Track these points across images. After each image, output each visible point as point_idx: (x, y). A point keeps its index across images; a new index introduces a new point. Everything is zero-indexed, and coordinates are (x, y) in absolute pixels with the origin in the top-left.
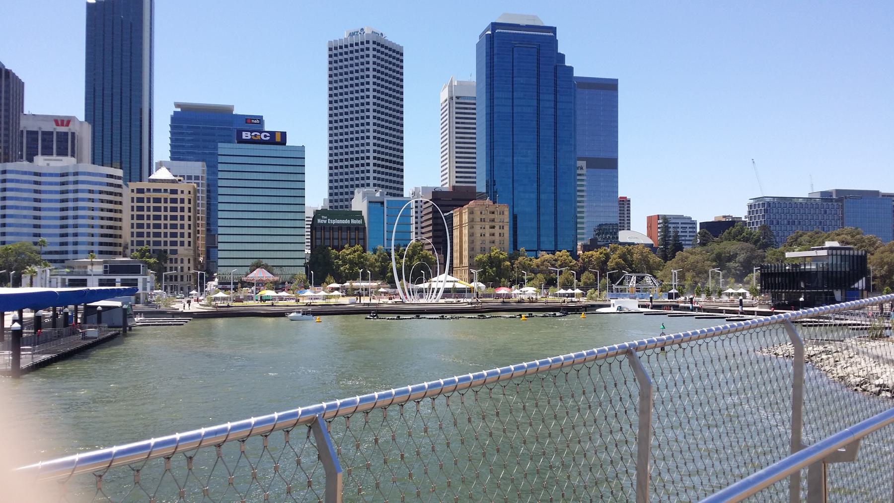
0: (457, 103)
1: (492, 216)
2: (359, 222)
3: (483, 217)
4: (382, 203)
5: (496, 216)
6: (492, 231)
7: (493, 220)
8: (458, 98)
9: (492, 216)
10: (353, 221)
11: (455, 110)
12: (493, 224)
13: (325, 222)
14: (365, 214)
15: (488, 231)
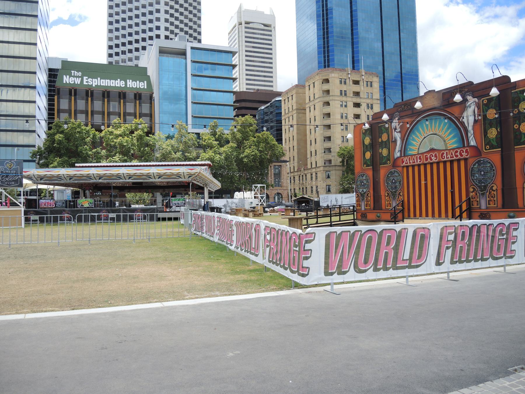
0: (246, 28)
1: (356, 88)
2: (142, 85)
3: (344, 88)
4: (183, 53)
5: (361, 88)
6: (357, 111)
7: (357, 94)
8: (247, 23)
9: (356, 88)
10: (131, 84)
11: (244, 34)
12: (357, 100)
13: (78, 81)
14: (152, 72)
15: (351, 111)
